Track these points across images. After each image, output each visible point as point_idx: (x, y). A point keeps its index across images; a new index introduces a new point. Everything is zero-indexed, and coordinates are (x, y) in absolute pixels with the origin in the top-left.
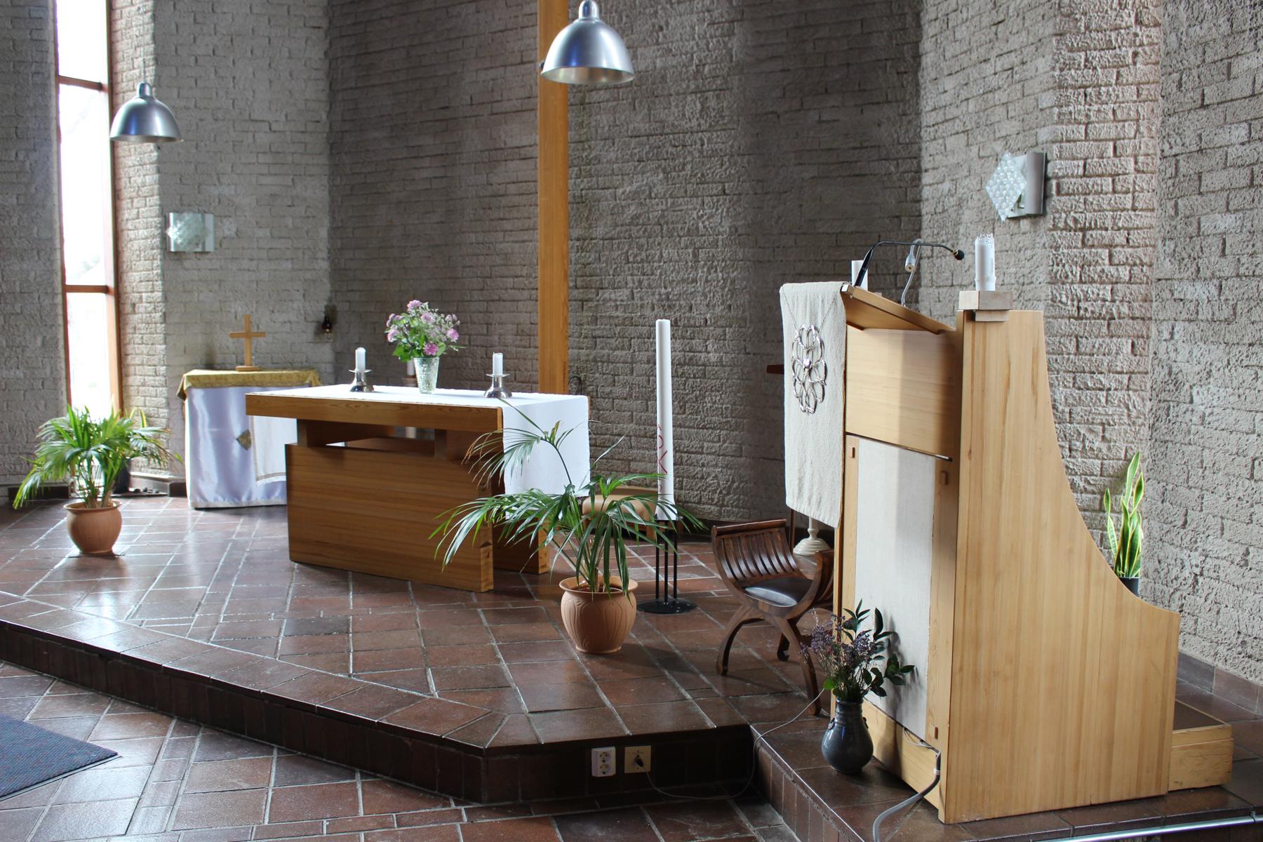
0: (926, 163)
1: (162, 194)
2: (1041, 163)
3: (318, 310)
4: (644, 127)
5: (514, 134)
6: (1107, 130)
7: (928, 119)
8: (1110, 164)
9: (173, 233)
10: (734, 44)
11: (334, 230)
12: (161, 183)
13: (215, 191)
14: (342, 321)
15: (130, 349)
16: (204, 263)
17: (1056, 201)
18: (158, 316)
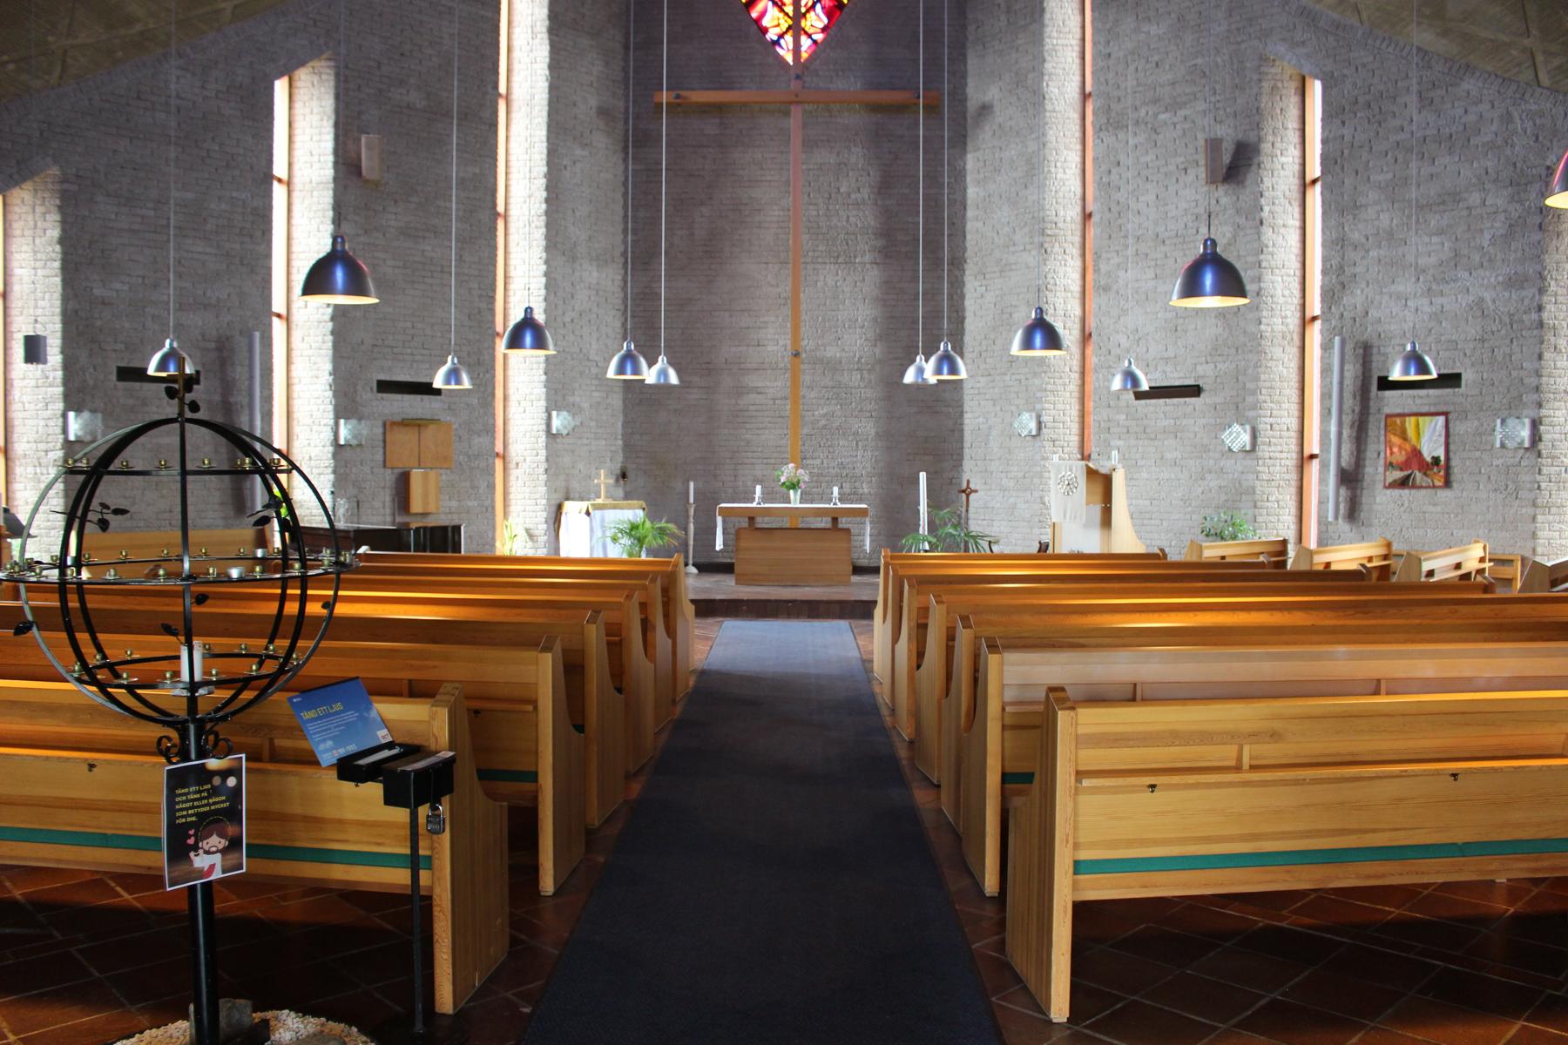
0: (966, 408)
1: (548, 399)
2: (1039, 417)
3: (617, 467)
4: (830, 384)
5: (753, 381)
6: (1060, 407)
7: (966, 392)
8: (1062, 418)
9: (557, 423)
10: (878, 351)
11: (625, 424)
12: (547, 394)
13: (571, 399)
14: (631, 475)
15: (512, 490)
16: (566, 441)
17: (1044, 430)
18: (542, 470)
